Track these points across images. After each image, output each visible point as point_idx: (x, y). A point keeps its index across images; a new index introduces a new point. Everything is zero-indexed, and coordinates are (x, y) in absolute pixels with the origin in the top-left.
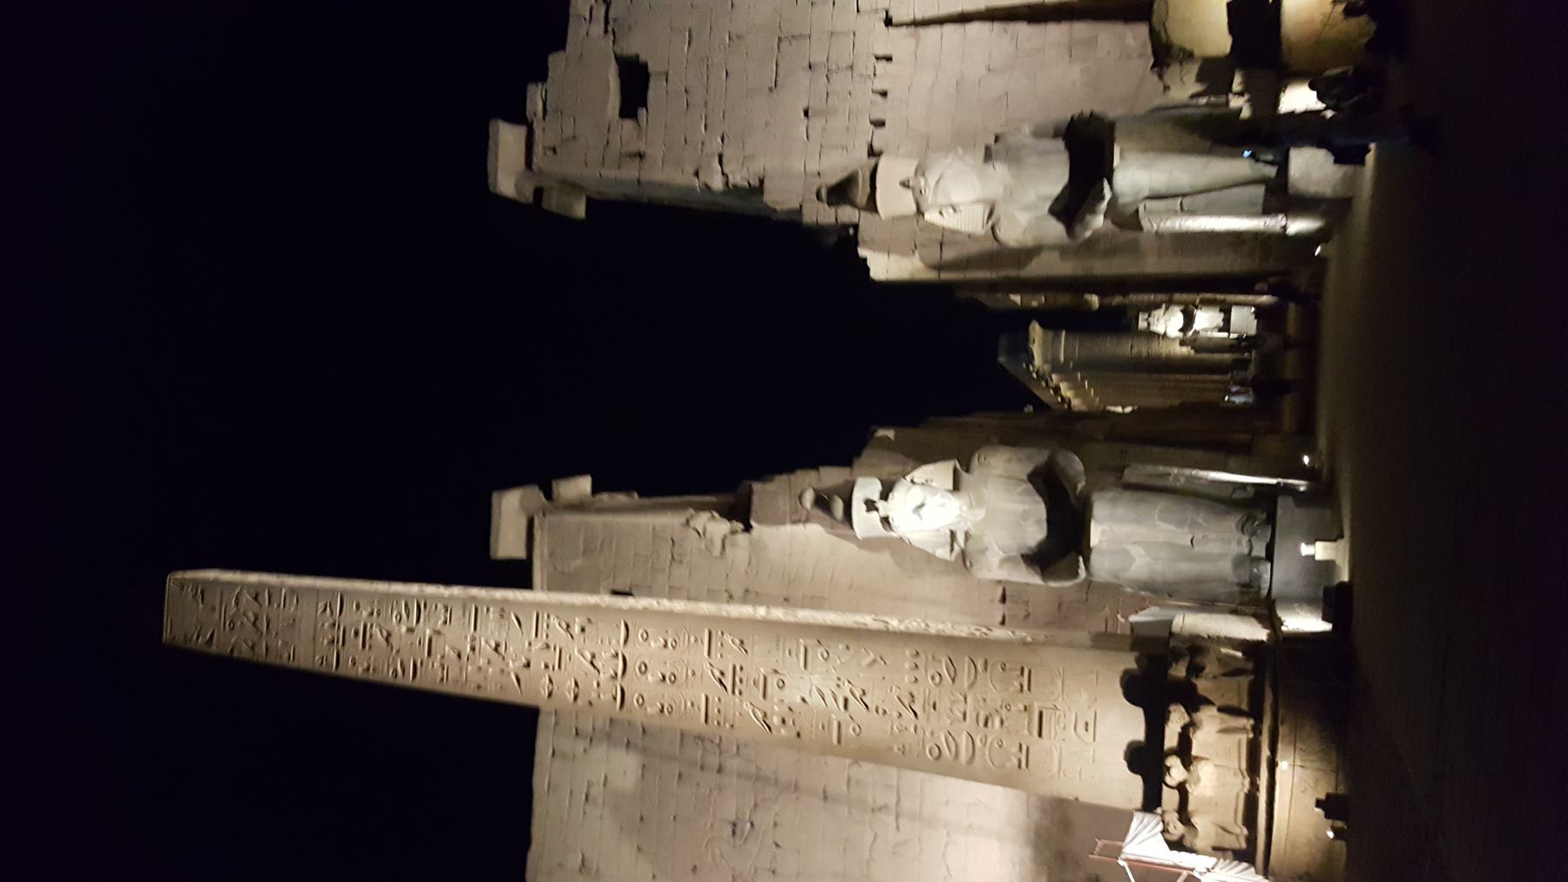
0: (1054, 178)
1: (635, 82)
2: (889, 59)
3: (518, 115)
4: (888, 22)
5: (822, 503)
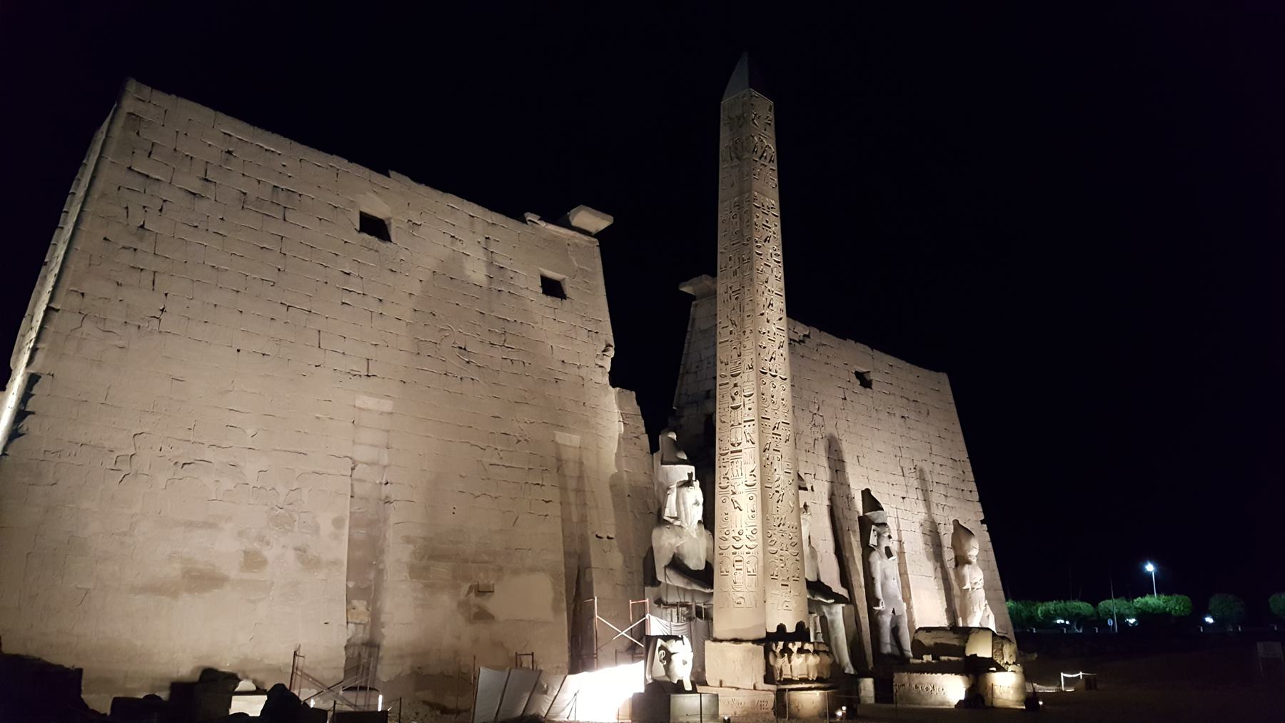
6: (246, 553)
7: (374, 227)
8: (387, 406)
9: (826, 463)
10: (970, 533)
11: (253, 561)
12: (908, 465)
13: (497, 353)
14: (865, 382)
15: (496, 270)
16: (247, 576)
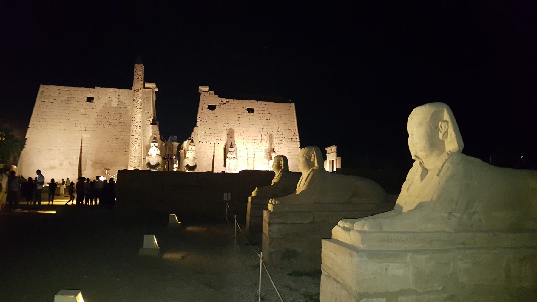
0: (191, 165)
3: (209, 90)
5: (155, 138)
7: (90, 100)
8: (89, 136)
9: (226, 136)
10: (274, 151)
11: (61, 165)
12: (264, 133)
13: (117, 122)
14: (251, 111)
15: (120, 102)
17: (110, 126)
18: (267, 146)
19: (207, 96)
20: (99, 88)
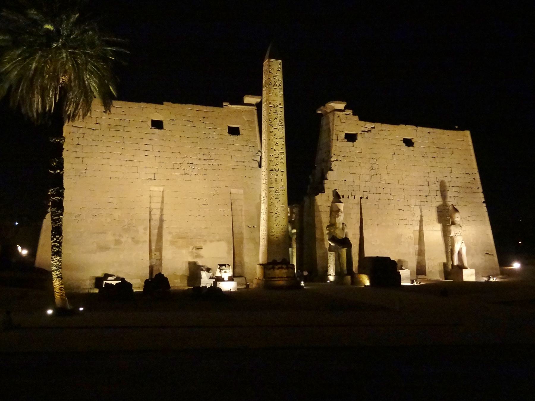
1: (351, 138)
2: (354, 198)
3: (346, 108)
4: (361, 198)
6: (116, 240)
7: (158, 125)
10: (456, 210)
13: (204, 162)
14: (409, 143)
16: (116, 247)
17: (195, 171)
18: (439, 201)
19: (341, 118)
20: (170, 104)
